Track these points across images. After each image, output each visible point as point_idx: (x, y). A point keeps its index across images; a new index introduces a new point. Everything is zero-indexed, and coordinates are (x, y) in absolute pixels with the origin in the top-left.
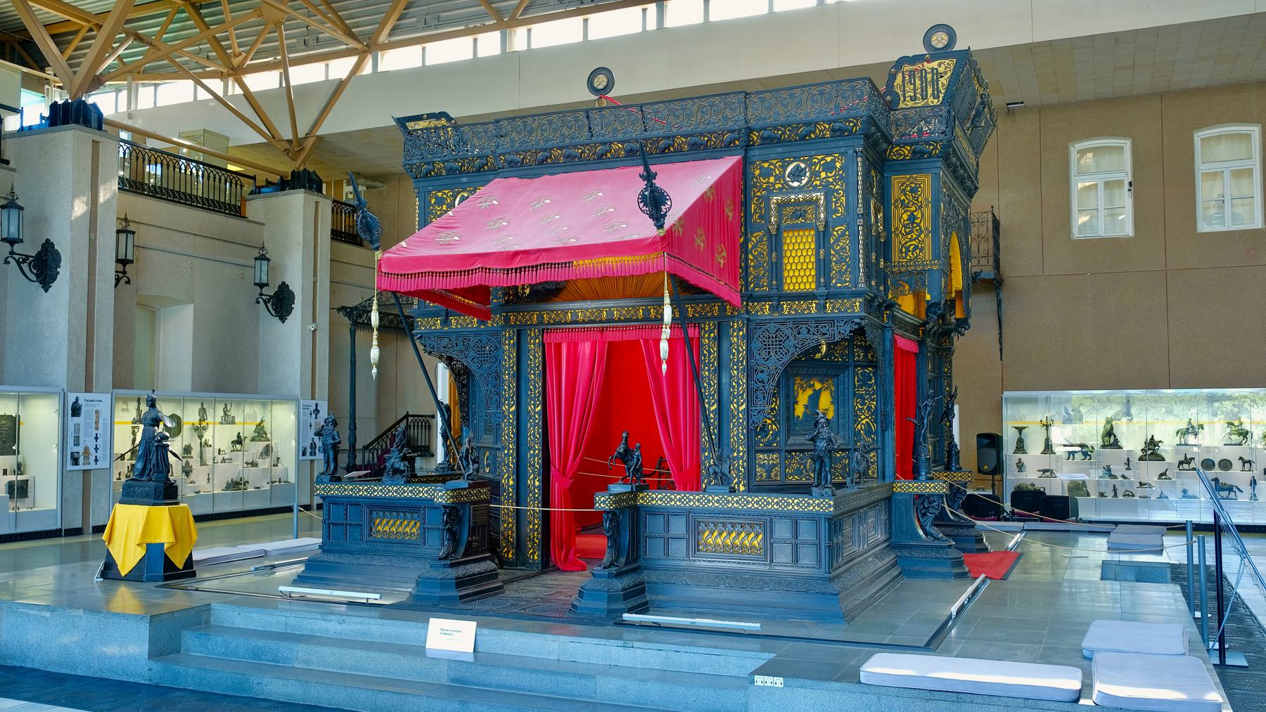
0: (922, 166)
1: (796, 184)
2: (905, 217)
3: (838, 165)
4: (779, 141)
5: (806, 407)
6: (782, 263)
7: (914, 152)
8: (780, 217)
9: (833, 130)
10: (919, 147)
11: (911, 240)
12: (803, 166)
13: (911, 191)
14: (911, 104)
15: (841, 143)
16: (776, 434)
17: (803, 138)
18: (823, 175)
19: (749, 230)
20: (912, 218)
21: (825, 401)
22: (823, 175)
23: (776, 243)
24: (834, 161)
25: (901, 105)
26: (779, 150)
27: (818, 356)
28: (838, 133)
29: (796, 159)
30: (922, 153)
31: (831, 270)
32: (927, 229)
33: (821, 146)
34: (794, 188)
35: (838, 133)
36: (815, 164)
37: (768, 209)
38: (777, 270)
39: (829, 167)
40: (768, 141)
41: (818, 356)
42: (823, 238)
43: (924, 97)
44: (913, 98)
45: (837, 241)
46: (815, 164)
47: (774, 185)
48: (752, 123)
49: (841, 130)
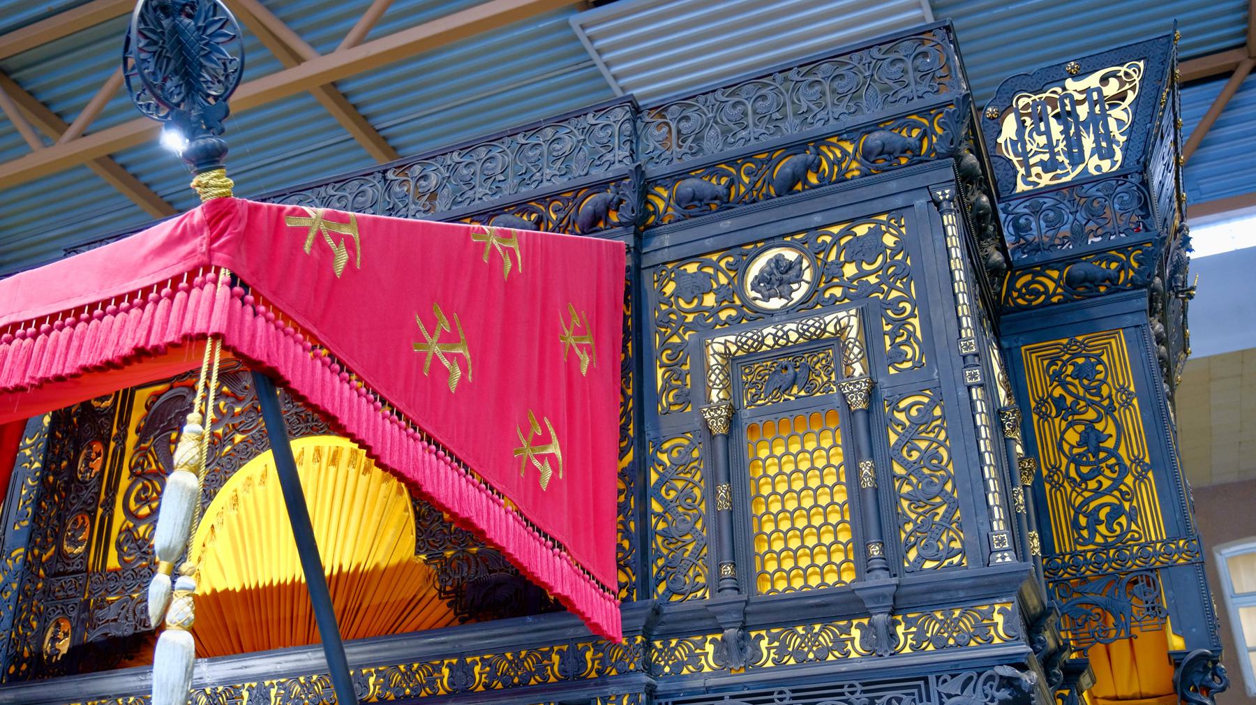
0: (1096, 312)
1: (776, 303)
2: (1072, 437)
3: (889, 240)
4: (725, 203)
6: (747, 517)
7: (1071, 282)
8: (732, 384)
9: (867, 154)
10: (1079, 269)
11: (1098, 493)
12: (791, 255)
13: (1078, 374)
14: (1046, 180)
15: (893, 186)
17: (790, 190)
18: (850, 270)
19: (650, 433)
20: (1091, 438)
22: (850, 270)
23: (727, 454)
24: (877, 234)
25: (1021, 187)
26: (726, 225)
28: (880, 160)
29: (771, 241)
30: (1091, 282)
31: (901, 520)
32: (1137, 461)
33: (838, 199)
34: (771, 313)
35: (880, 160)
36: (826, 248)
37: (702, 369)
38: (735, 534)
39: (862, 251)
40: (694, 207)
42: (865, 428)
43: (1076, 158)
44: (1047, 167)
45: (908, 440)
46: (826, 248)
47: (714, 312)
48: (652, 170)
49: (885, 151)
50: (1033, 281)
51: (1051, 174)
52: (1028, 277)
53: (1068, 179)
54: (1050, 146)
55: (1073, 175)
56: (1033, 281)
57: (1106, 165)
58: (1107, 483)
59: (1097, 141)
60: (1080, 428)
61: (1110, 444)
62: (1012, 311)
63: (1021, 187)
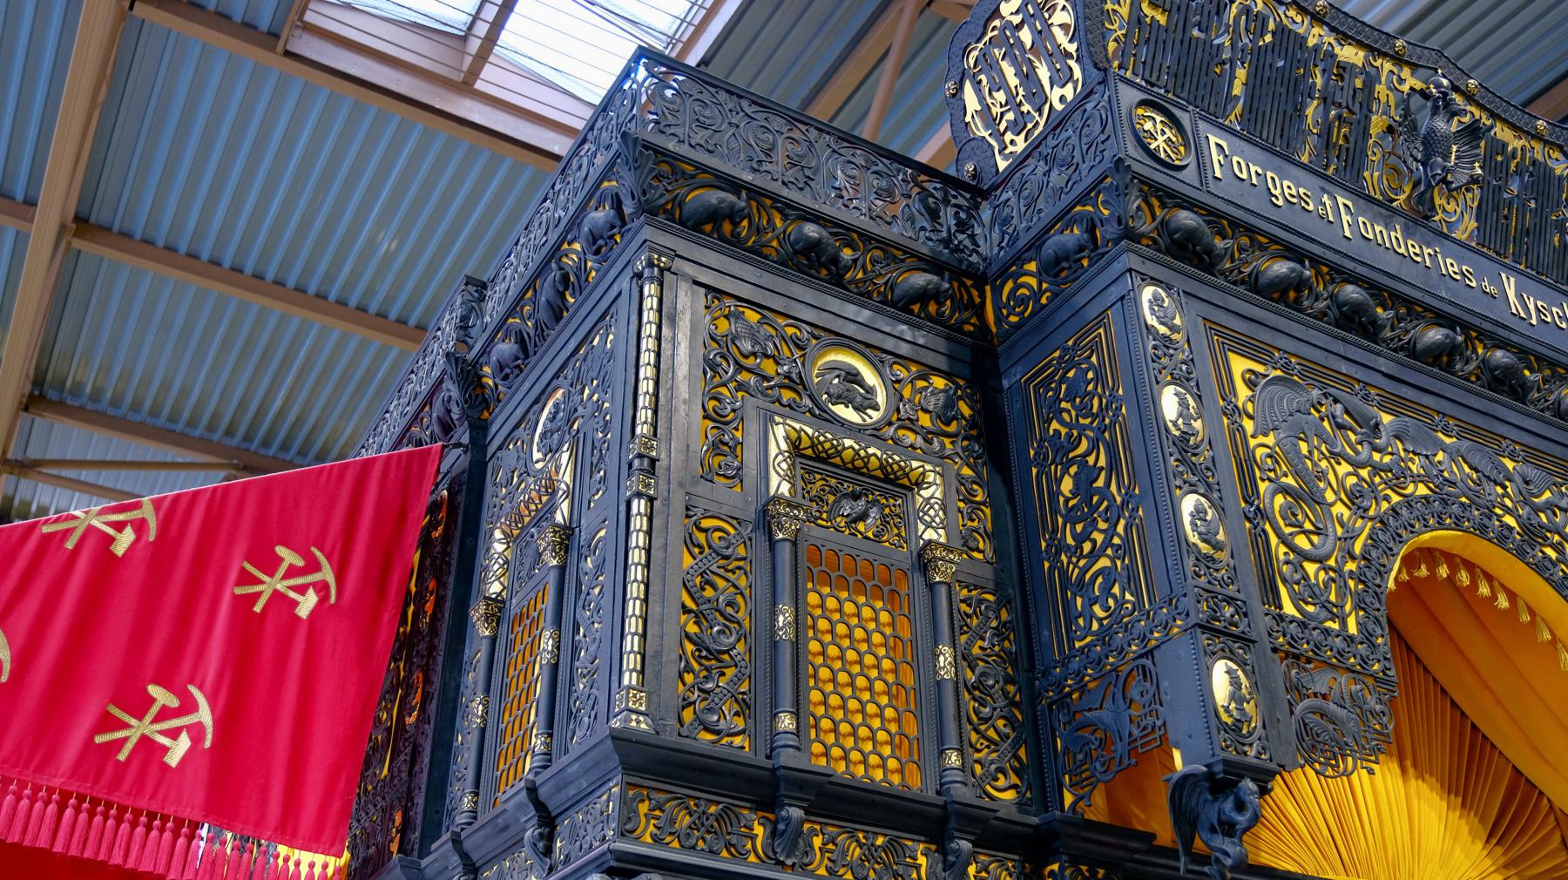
2: (1067, 485)
7: (1053, 269)
11: (1094, 555)
25: (1002, 165)
43: (1038, 97)
50: (1017, 287)
51: (1023, 134)
52: (1009, 285)
53: (1040, 128)
54: (1011, 97)
55: (1042, 123)
56: (1017, 287)
57: (1069, 92)
58: (1099, 537)
59: (1051, 67)
60: (1073, 470)
61: (1100, 483)
62: (1008, 335)
63: (1002, 165)
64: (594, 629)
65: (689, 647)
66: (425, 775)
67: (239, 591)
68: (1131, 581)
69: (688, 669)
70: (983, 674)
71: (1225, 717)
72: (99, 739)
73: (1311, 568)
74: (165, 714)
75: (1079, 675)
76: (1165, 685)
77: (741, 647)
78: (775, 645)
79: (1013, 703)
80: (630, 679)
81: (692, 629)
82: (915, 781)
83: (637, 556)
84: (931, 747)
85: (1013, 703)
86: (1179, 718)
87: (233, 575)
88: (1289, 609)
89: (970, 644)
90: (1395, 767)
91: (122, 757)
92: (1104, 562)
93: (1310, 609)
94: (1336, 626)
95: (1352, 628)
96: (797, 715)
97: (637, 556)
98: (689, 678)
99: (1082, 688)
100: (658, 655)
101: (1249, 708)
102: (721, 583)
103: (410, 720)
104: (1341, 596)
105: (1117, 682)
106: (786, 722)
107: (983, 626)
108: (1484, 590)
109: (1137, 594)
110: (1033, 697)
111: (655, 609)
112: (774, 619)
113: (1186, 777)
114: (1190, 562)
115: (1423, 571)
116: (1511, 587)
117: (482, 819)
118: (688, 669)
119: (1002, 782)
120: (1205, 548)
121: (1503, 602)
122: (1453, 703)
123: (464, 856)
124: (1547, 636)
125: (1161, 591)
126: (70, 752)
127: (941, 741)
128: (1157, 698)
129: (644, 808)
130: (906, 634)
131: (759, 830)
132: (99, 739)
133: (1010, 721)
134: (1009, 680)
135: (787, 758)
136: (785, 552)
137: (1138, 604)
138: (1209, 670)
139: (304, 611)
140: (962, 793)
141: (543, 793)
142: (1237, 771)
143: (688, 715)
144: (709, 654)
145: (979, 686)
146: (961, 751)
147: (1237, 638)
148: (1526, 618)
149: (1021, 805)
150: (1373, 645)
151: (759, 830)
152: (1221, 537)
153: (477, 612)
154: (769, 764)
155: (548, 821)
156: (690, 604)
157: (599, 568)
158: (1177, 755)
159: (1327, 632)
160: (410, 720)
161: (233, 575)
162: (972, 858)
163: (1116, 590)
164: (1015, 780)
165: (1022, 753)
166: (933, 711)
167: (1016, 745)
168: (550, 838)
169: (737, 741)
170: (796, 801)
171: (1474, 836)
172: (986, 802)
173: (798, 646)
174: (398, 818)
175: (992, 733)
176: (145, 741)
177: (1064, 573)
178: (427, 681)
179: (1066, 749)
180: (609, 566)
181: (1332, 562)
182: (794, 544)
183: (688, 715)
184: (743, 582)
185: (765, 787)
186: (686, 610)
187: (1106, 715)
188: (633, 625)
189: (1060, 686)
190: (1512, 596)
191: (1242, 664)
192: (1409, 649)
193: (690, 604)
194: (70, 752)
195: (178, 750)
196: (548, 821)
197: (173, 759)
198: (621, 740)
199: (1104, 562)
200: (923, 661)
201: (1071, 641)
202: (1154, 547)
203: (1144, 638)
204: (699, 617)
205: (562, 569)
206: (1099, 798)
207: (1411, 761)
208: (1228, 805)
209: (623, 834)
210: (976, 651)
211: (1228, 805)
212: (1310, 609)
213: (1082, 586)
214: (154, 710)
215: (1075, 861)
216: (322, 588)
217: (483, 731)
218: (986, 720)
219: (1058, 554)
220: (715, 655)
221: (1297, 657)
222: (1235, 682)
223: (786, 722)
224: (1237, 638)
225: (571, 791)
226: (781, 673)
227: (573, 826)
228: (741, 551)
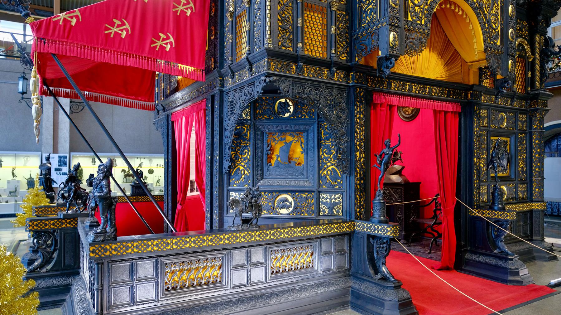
5: (278, 156)
11: (369, 5)
16: (248, 178)
21: (298, 152)
27: (287, 115)
41: (287, 115)
64: (258, 23)
65: (280, 28)
66: (218, 51)
67: (174, 10)
68: (376, 12)
69: (280, 33)
70: (341, 32)
71: (391, 45)
72: (152, 46)
73: (417, 8)
74: (164, 40)
75: (362, 33)
76: (380, 37)
77: (290, 28)
78: (297, 27)
79: (347, 38)
80: (268, 36)
81: (280, 24)
82: (325, 56)
83: (268, 7)
84: (329, 49)
85: (347, 38)
86: (382, 45)
87: (172, 6)
88: (410, 19)
89: (339, 24)
90: (428, 50)
91: (157, 49)
92: (371, 7)
93: (415, 18)
94: (419, 22)
95: (423, 23)
96: (302, 43)
97: (268, 7)
98: (280, 35)
99: (362, 35)
100: (273, 31)
101: (396, 43)
102: (286, 13)
103: (212, 38)
104: (422, 15)
105: (370, 35)
106: (300, 45)
107: (342, 20)
108: (457, 10)
109: (377, 15)
110: (351, 36)
111: (273, 20)
112: (297, 21)
113: (381, 57)
114: (389, 9)
115: (444, 6)
116: (464, 9)
117: (234, 64)
118: (280, 33)
119: (343, 56)
120: (393, 5)
121: (460, 13)
122: (445, 34)
123: (231, 70)
124: (468, 21)
125: (382, 15)
126: (147, 49)
127: (331, 47)
128: (378, 39)
129: (272, 64)
130: (325, 23)
131: (294, 67)
132: (152, 46)
133: (346, 42)
134: (347, 33)
135: (300, 53)
136: (300, 5)
137: (377, 18)
138: (389, 34)
139: (188, 14)
140: (335, 59)
141: (250, 59)
142: (391, 56)
143: (280, 44)
144: (284, 29)
145: (340, 34)
146: (335, 50)
147: (396, 27)
148: (465, 16)
149: (347, 60)
150: (427, 26)
151: (294, 67)
152: (397, 2)
153: (228, 15)
154: (296, 54)
155: (251, 65)
156: (280, 19)
157: (259, 9)
158: (380, 52)
159: (417, 24)
160: (212, 38)
161: (172, 6)
162: (336, 72)
163: (373, 14)
164: (346, 55)
165: (348, 49)
166: (330, 41)
167: (347, 48)
168: (251, 68)
169: (290, 49)
170: (301, 61)
171: (442, 64)
172: (339, 61)
173: (302, 28)
174: (213, 60)
175: (342, 45)
176: (161, 46)
177: (362, 8)
178: (216, 29)
179: (357, 49)
180: (262, 7)
181: (422, 7)
182: (302, 3)
183: (280, 44)
184: (291, 12)
185: (295, 59)
186: (279, 20)
187: (367, 42)
188: (268, 24)
189: (358, 34)
190: (463, 11)
191: (397, 33)
192: (439, 21)
193: (280, 19)
194: (147, 49)
195: (168, 47)
196: (251, 65)
197: (168, 49)
198: (267, 50)
199: (371, 7)
200: (329, 29)
201: (361, 24)
202: (382, 4)
203: (377, 26)
204: (281, 21)
205: (249, 7)
206: (363, 59)
207: (432, 48)
208: (388, 63)
209: (268, 69)
210: (340, 26)
211: (388, 63)
212: (415, 18)
213: (365, 12)
214: (161, 39)
215: (356, 72)
216: (191, 8)
217: (232, 43)
218: (340, 42)
219: (361, 3)
220: (285, 30)
221: (409, 30)
222: (394, 37)
223: (300, 45)
224: (396, 27)
225: (256, 59)
226: (298, 33)
227: (256, 66)
228: (290, 5)
